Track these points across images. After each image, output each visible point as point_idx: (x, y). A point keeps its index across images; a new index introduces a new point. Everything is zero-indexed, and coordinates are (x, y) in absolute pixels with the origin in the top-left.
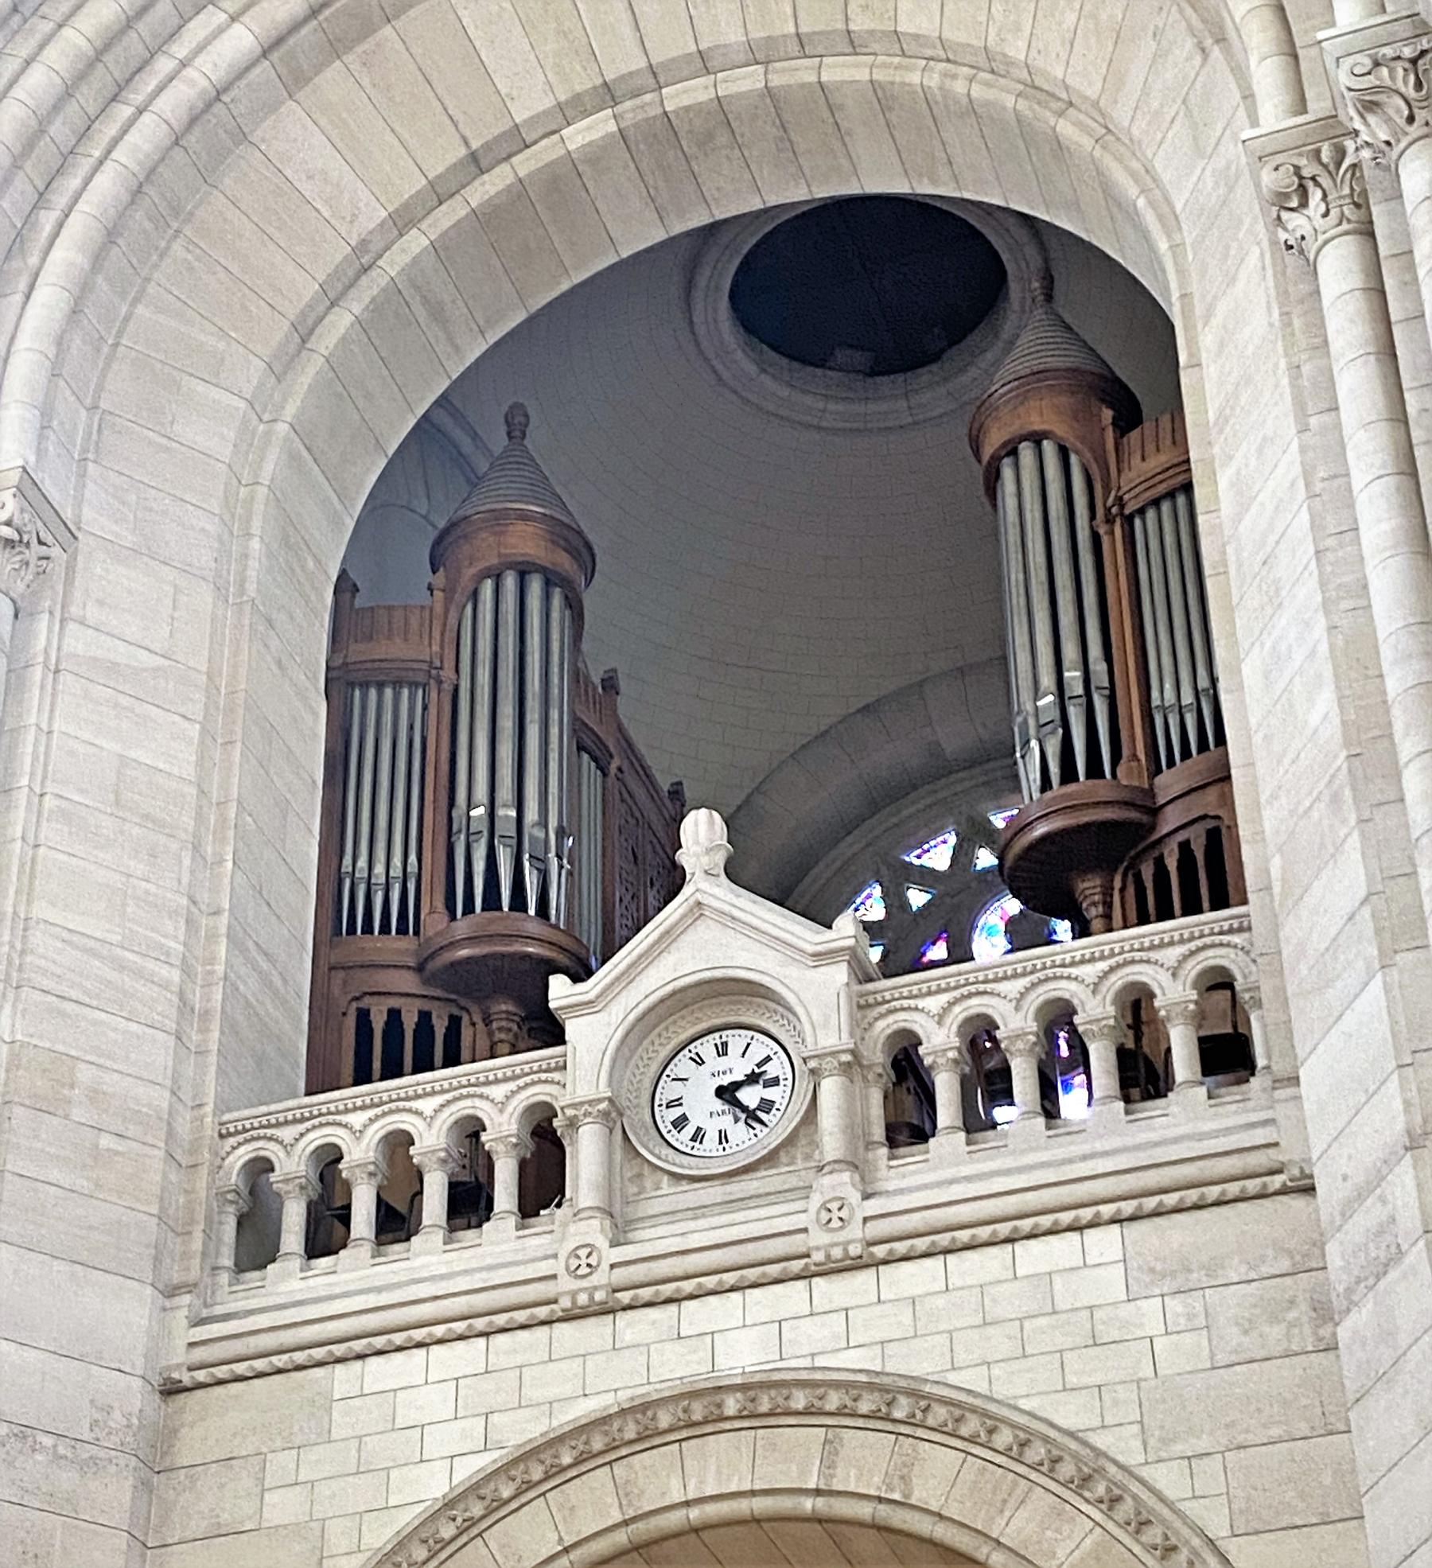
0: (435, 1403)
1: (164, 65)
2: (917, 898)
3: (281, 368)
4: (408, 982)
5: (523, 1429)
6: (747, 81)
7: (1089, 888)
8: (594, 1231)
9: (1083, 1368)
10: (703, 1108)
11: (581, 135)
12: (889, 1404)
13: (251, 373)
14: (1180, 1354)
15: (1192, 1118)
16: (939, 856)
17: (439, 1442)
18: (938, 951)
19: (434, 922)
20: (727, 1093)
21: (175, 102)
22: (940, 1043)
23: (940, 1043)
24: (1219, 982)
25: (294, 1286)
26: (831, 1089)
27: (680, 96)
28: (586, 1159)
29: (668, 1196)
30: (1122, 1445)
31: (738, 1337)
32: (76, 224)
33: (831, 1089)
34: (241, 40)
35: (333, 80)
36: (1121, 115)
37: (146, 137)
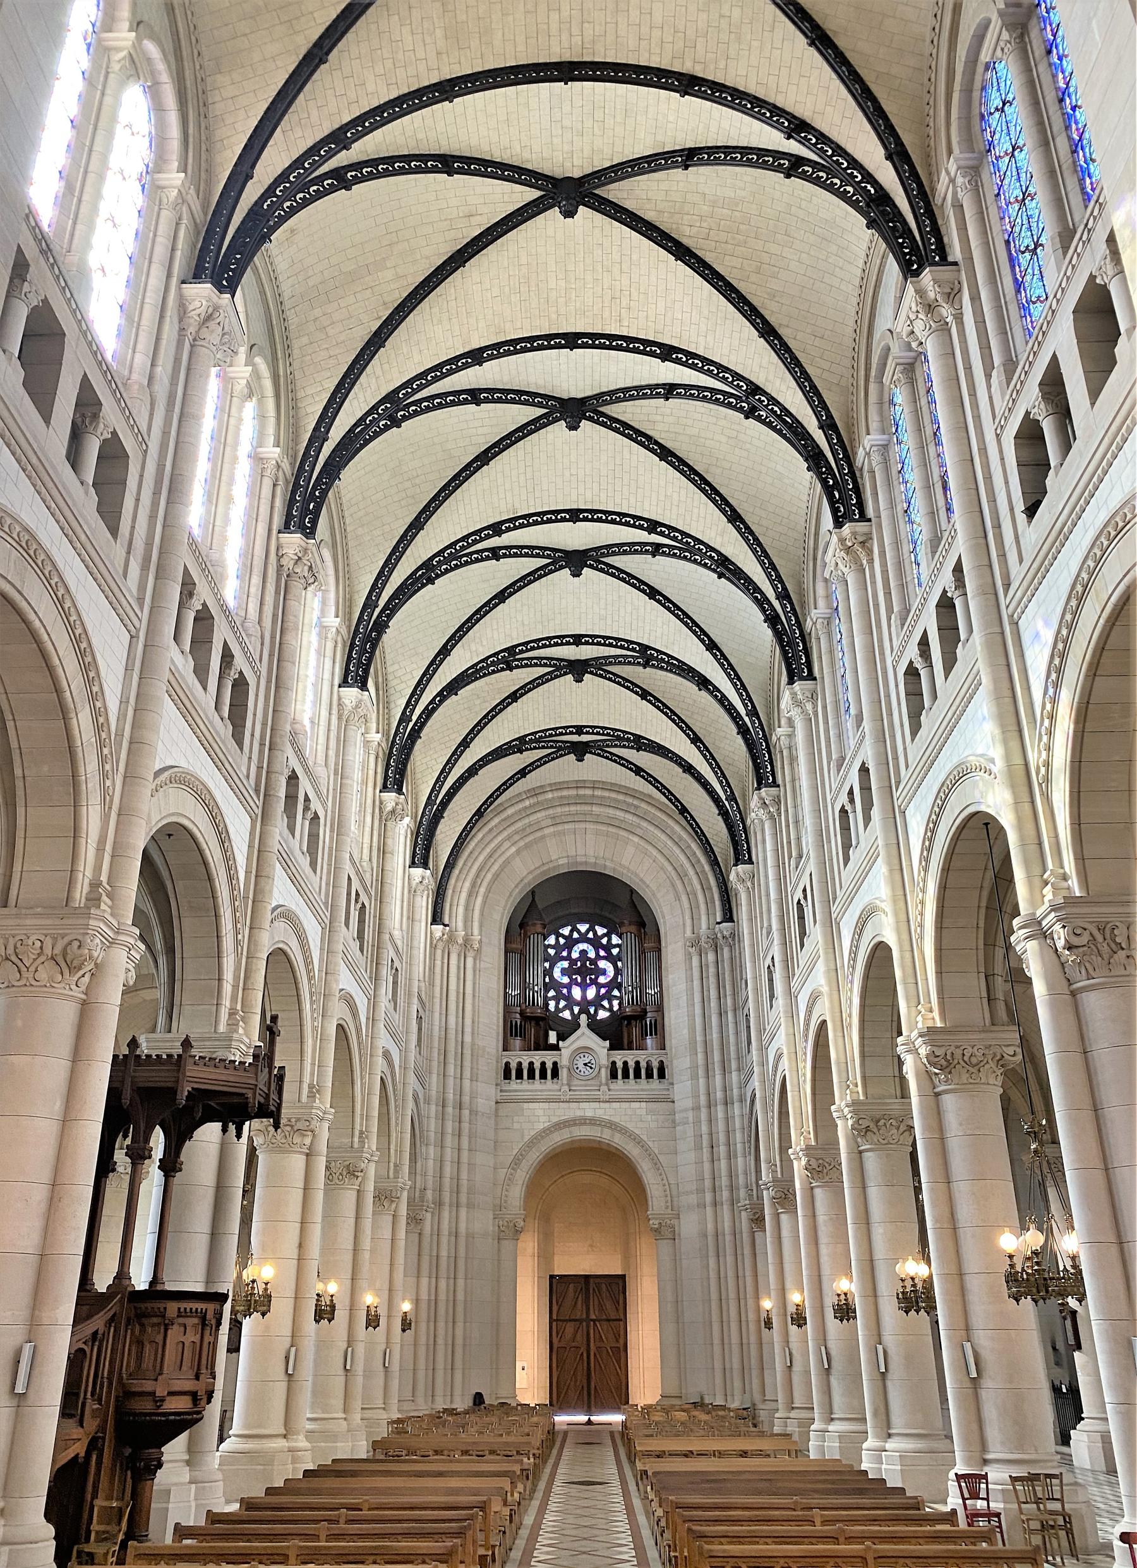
0: (541, 1112)
1: (499, 852)
2: (562, 941)
3: (507, 901)
4: (518, 1016)
5: (555, 1120)
6: (593, 860)
7: (633, 1023)
8: (566, 1088)
9: (640, 1125)
10: (581, 1066)
11: (561, 862)
12: (612, 1126)
13: (503, 903)
14: (653, 1125)
15: (655, 1083)
16: (566, 931)
17: (542, 1119)
18: (565, 954)
19: (524, 1007)
20: (585, 1064)
21: (501, 861)
22: (620, 1065)
23: (620, 1065)
24: (661, 1063)
25: (514, 1084)
26: (603, 1071)
27: (579, 859)
28: (563, 1073)
29: (576, 1082)
30: (644, 1138)
31: (589, 1110)
32: (485, 884)
33: (603, 1071)
34: (513, 849)
35: (524, 853)
36: (659, 895)
37: (496, 867)
